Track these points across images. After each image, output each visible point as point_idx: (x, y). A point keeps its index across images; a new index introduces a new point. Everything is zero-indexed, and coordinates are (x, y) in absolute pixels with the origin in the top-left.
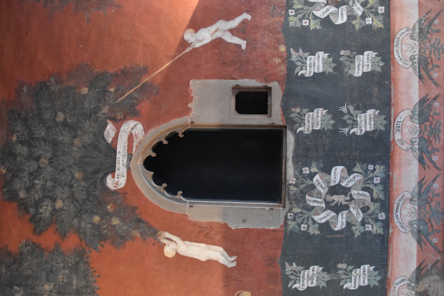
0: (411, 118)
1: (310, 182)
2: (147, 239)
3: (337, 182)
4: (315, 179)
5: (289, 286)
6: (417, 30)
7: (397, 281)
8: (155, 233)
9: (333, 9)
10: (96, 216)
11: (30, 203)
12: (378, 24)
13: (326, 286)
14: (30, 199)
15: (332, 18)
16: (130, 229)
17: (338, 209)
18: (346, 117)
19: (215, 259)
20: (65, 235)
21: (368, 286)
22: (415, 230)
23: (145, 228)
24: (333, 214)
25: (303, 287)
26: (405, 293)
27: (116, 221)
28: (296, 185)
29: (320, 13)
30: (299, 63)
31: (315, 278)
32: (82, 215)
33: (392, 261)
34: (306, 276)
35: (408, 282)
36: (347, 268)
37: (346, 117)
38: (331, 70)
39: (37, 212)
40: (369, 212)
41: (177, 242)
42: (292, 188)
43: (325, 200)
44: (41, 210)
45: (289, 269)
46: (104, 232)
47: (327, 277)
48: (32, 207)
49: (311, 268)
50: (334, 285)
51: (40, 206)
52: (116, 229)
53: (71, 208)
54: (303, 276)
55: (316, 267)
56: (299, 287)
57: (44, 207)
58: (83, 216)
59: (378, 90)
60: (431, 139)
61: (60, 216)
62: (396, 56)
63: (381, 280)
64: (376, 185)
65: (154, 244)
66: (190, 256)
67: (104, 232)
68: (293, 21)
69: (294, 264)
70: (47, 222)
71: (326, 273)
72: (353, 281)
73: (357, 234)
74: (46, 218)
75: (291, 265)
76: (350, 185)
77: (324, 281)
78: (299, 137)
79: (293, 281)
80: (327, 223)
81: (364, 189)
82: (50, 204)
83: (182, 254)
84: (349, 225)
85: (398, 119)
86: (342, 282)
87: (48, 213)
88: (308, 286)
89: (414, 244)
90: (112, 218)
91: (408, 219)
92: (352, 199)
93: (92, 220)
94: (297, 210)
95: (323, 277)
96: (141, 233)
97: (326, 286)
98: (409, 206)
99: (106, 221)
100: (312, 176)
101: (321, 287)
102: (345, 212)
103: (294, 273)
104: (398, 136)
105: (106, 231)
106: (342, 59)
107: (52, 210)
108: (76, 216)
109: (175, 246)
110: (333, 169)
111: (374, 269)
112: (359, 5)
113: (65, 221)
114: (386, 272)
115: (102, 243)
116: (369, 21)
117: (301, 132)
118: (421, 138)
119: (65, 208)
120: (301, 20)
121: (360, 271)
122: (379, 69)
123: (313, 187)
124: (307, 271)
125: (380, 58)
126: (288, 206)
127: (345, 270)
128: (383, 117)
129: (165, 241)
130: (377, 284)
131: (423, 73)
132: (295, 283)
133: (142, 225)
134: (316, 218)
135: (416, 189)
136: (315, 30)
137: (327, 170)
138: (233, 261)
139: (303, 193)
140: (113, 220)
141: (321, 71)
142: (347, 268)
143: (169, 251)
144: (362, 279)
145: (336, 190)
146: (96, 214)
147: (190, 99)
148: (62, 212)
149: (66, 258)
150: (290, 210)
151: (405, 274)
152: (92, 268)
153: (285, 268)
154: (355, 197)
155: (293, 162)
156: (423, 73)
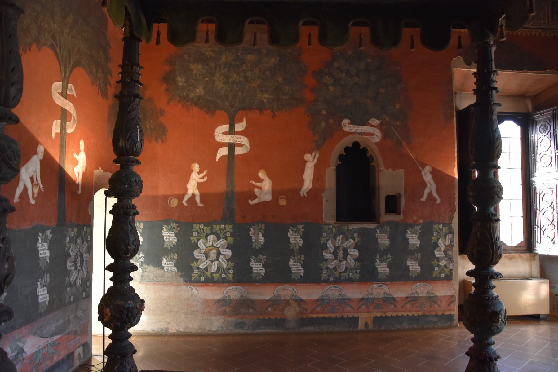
0: (385, 293)
1: (350, 237)
3: (350, 253)
4: (351, 240)
6: (431, 295)
8: (318, 148)
9: (443, 249)
12: (435, 274)
15: (438, 248)
17: (335, 254)
18: (385, 257)
21: (292, 273)
22: (324, 298)
24: (332, 251)
27: (323, 124)
28: (348, 229)
29: (440, 242)
30: (413, 230)
37: (385, 257)
38: (410, 248)
40: (334, 271)
42: (346, 227)
43: (340, 246)
45: (301, 227)
47: (296, 249)
49: (301, 239)
50: (292, 253)
55: (302, 242)
59: (400, 275)
60: (374, 305)
62: (418, 284)
64: (348, 275)
68: (436, 227)
69: (303, 230)
73: (321, 265)
75: (303, 228)
76: (348, 260)
78: (374, 231)
80: (327, 248)
81: (346, 268)
84: (326, 260)
85: (384, 286)
89: (316, 298)
91: (330, 293)
92: (341, 261)
94: (334, 230)
98: (337, 293)
100: (353, 238)
102: (333, 258)
104: (375, 286)
106: (416, 254)
109: (311, 161)
110: (356, 250)
112: (445, 263)
114: (300, 283)
116: (436, 269)
117: (377, 232)
118: (374, 299)
120: (437, 231)
122: (411, 274)
123: (347, 239)
125: (417, 275)
126: (336, 225)
128: (385, 277)
129: (313, 154)
131: (409, 299)
134: (330, 242)
135: (346, 297)
136: (431, 239)
137: (356, 247)
139: (343, 234)
141: (410, 242)
143: (308, 157)
145: (346, 253)
147: (393, 169)
150: (334, 227)
154: (342, 263)
155: (360, 228)
156: (409, 299)
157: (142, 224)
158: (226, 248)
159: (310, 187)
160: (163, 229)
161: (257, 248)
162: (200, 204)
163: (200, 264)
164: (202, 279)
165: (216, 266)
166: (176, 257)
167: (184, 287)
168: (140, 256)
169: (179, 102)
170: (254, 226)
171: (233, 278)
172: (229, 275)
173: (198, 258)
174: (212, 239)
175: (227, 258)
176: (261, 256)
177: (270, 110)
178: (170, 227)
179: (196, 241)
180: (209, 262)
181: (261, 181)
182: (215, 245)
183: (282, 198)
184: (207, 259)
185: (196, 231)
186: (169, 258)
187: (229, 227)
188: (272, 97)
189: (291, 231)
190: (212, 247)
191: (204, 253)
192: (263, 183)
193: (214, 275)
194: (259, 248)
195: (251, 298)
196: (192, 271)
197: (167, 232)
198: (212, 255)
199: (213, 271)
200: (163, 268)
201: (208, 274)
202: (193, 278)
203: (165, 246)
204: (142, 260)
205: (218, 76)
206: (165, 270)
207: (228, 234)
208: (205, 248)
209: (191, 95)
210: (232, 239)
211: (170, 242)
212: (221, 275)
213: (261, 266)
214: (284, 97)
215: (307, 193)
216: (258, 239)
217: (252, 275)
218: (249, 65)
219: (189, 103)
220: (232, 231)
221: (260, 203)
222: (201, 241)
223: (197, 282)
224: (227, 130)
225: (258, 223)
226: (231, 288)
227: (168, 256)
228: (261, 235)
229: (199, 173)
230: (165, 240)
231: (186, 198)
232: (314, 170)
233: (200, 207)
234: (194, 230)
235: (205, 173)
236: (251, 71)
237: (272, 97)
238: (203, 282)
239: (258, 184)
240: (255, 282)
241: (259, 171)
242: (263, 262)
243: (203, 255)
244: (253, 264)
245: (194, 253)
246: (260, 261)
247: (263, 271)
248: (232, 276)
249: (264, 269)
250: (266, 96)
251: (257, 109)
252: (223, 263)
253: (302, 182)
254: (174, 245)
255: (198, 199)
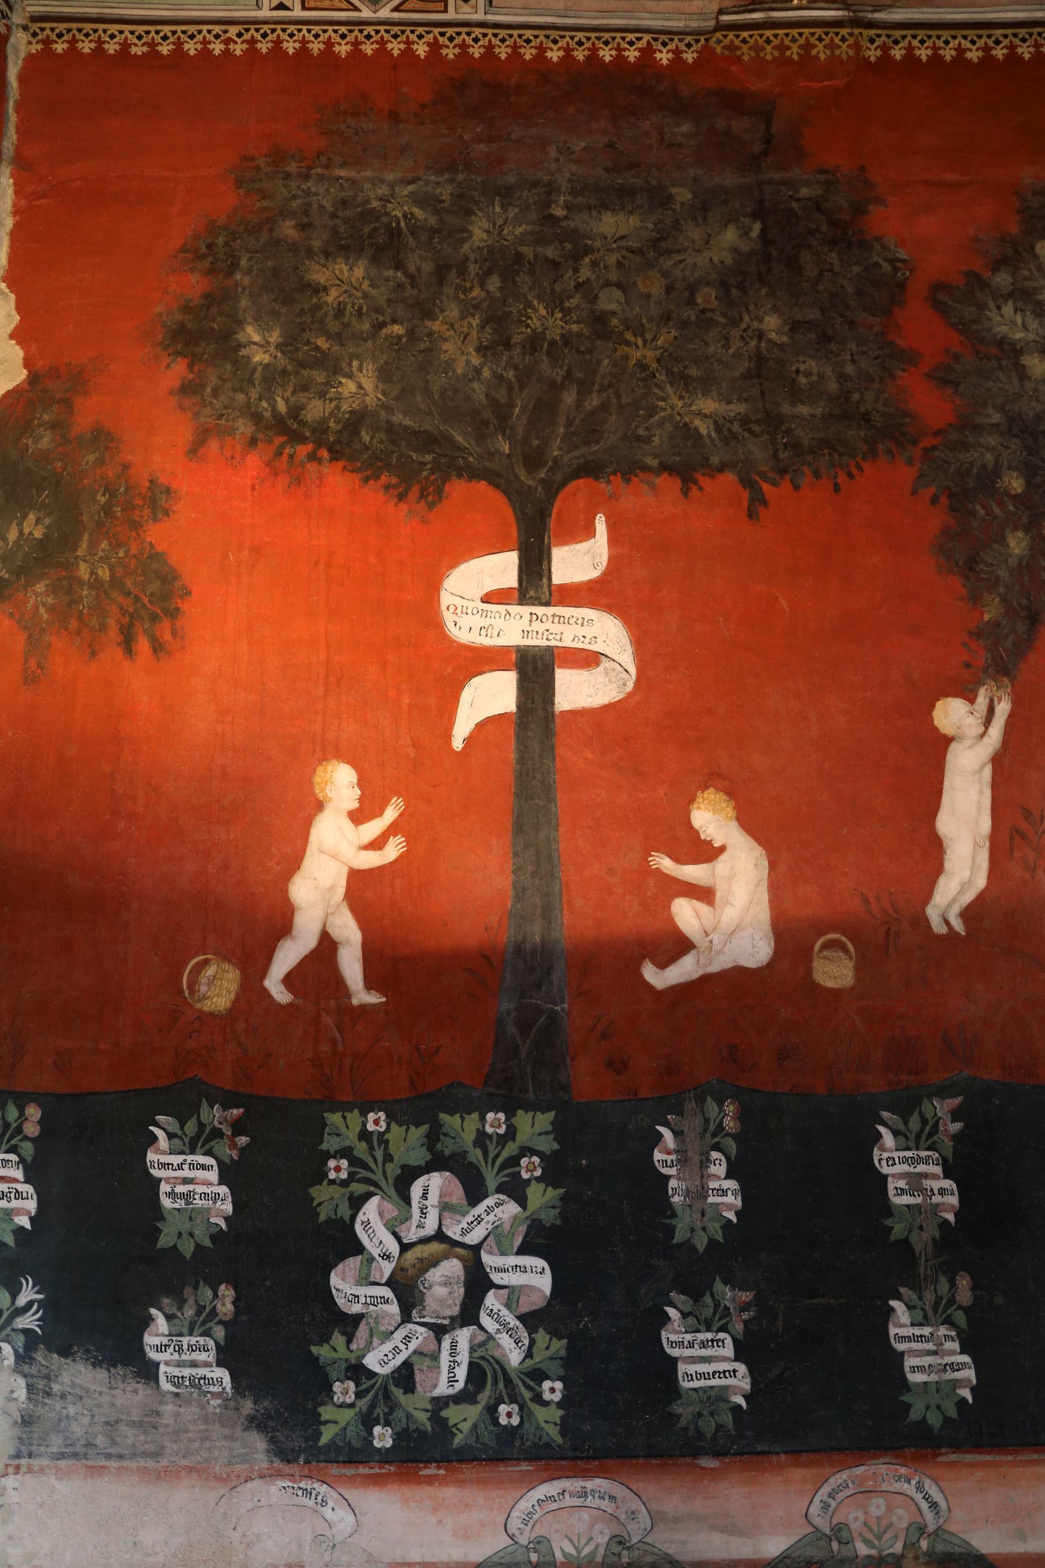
2: (981, 643)
5: (885, 1114)
7: (928, 1483)
8: (1002, 669)
10: (1021, 481)
11: (1026, 273)
13: (892, 1238)
14: (1036, 273)
16: (1001, 590)
19: (947, 865)
20: (945, 382)
21: (905, 1385)
23: (1012, 637)
25: (884, 1163)
26: (895, 1519)
27: (1017, 544)
31: (919, 1200)
32: (1017, 436)
33: (997, 1465)
34: (921, 1168)
35: (931, 1528)
36: (960, 1307)
39: (1002, 296)
41: (986, 739)
44: (1008, 309)
45: (941, 1108)
46: (978, 507)
47: (922, 1241)
48: (1014, 279)
49: (948, 1184)
51: (1020, 305)
52: (995, 546)
53: (1034, 404)
54: (920, 1160)
55: (954, 1200)
56: (883, 1149)
57: (1019, 319)
58: (1015, 440)
61: (1000, 368)
63: (930, 1428)
65: (968, 665)
66: (946, 784)
67: (978, 507)
69: (957, 1126)
70: (975, 327)
71: (937, 1235)
72: (917, 1331)
74: (987, 325)
75: (955, 1116)
77: (910, 1230)
79: (902, 1128)
82: (1032, 337)
83: (948, 757)
86: (910, 1292)
87: (1004, 329)
88: (890, 1179)
90: (1027, 532)
93: (1009, 468)
95: (921, 1228)
96: (998, 626)
97: (892, 1238)
99: (1013, 514)
101: (889, 1222)
103: (928, 1128)
105: (982, 512)
107: (1013, 344)
108: (1012, 420)
111: (964, 1400)
113: (990, 384)
114: (957, 1446)
115: (944, 500)
119: (1029, 385)
121: (952, 1353)
124: (938, 1170)
127: (952, 1301)
129: (982, 700)
130: (914, 1415)
132: (896, 1133)
133: (1021, 627)
138: (947, 923)
140: (1020, 534)
142: (960, 1307)
143: (952, 714)
144: (926, 1361)
146: (1028, 483)
148: (1013, 374)
149: (876, 386)
151: (958, 1514)
152: (859, 467)
153: (943, 1098)
157: (34, 1112)
158: (522, 1251)
159: (981, 882)
160: (154, 1139)
161: (701, 1243)
162: (362, 996)
163: (369, 1347)
164: (383, 1437)
165: (464, 1358)
166: (226, 1307)
167: (276, 1492)
168: (22, 1300)
169: (253, 442)
170: (680, 1113)
171: (564, 1427)
172: (541, 1414)
173: (356, 1309)
174: (433, 1198)
175: (524, 1309)
176: (727, 1294)
177: (730, 476)
178: (191, 1127)
179: (344, 1211)
180: (421, 1336)
181: (706, 852)
182: (453, 1232)
183: (826, 946)
184: (406, 1317)
185: (346, 1153)
186: (189, 1312)
187: (535, 1127)
188: (738, 408)
189: (888, 1139)
190: (436, 1247)
191: (389, 1284)
192: (721, 865)
193: (452, 1414)
194: (712, 1243)
195: (672, 1550)
196: (320, 1386)
197: (176, 1159)
198: (441, 1291)
199: (443, 1389)
200: (148, 1372)
201: (415, 1407)
202: (327, 1434)
203: (165, 1241)
204: (29, 1321)
205: (453, 312)
206: (165, 1386)
207: (530, 1168)
208: (394, 1248)
209: (315, 410)
210: (553, 1194)
211: (192, 1215)
212: (492, 1411)
213: (729, 1350)
214: (804, 410)
215: (966, 914)
216: (702, 1193)
217: (677, 1409)
218: (612, 259)
219: (303, 450)
220: (548, 1145)
221: (706, 979)
222: (371, 1210)
223: (352, 1457)
224: (511, 580)
225: (701, 1100)
226: (551, 1488)
227: (182, 1302)
228: (719, 1168)
229: (358, 817)
230: (166, 1203)
231: (288, 956)
232: (995, 785)
233: (363, 1007)
234: (330, 1144)
235: (391, 814)
236: (619, 285)
237: (738, 408)
238: (386, 1457)
239: (692, 873)
240: (696, 1453)
241: (692, 800)
242: (739, 1327)
243: (387, 1292)
244: (675, 1338)
245: (335, 1280)
246: (714, 1321)
247: (739, 1381)
248: (557, 1414)
249: (742, 1368)
250: (710, 405)
251: (665, 468)
252: (505, 1341)
253: (933, 853)
254: (217, 1236)
255: (351, 966)
